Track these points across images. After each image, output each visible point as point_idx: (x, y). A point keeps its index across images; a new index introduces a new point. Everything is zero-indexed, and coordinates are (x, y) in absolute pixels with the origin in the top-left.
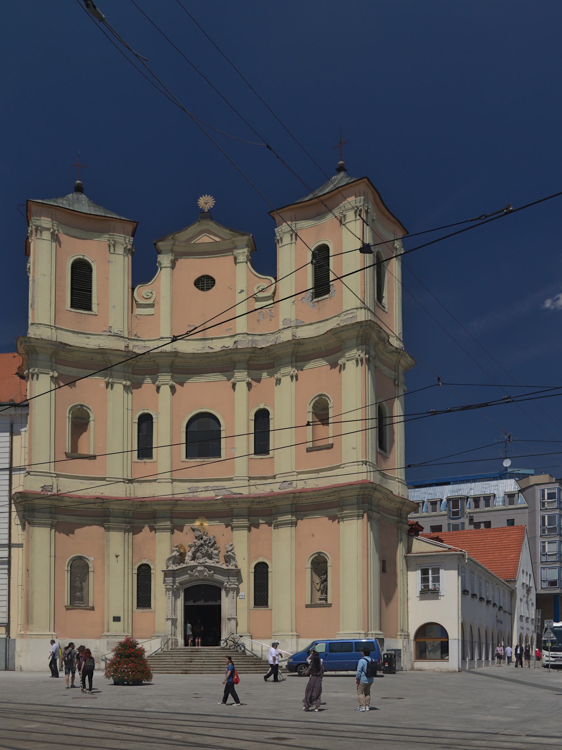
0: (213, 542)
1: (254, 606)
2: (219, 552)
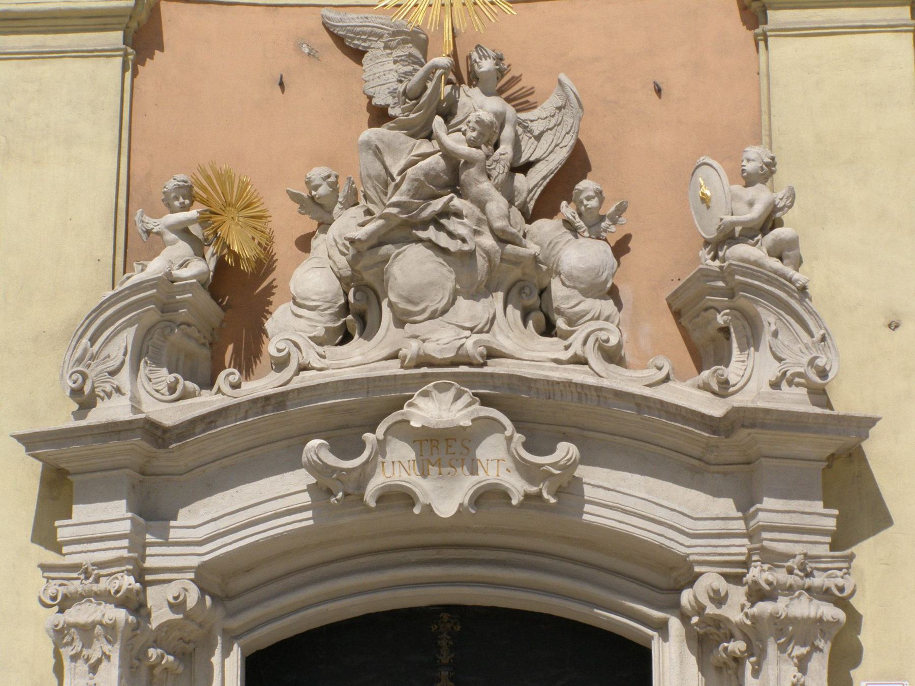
0: (561, 155)
2: (621, 248)
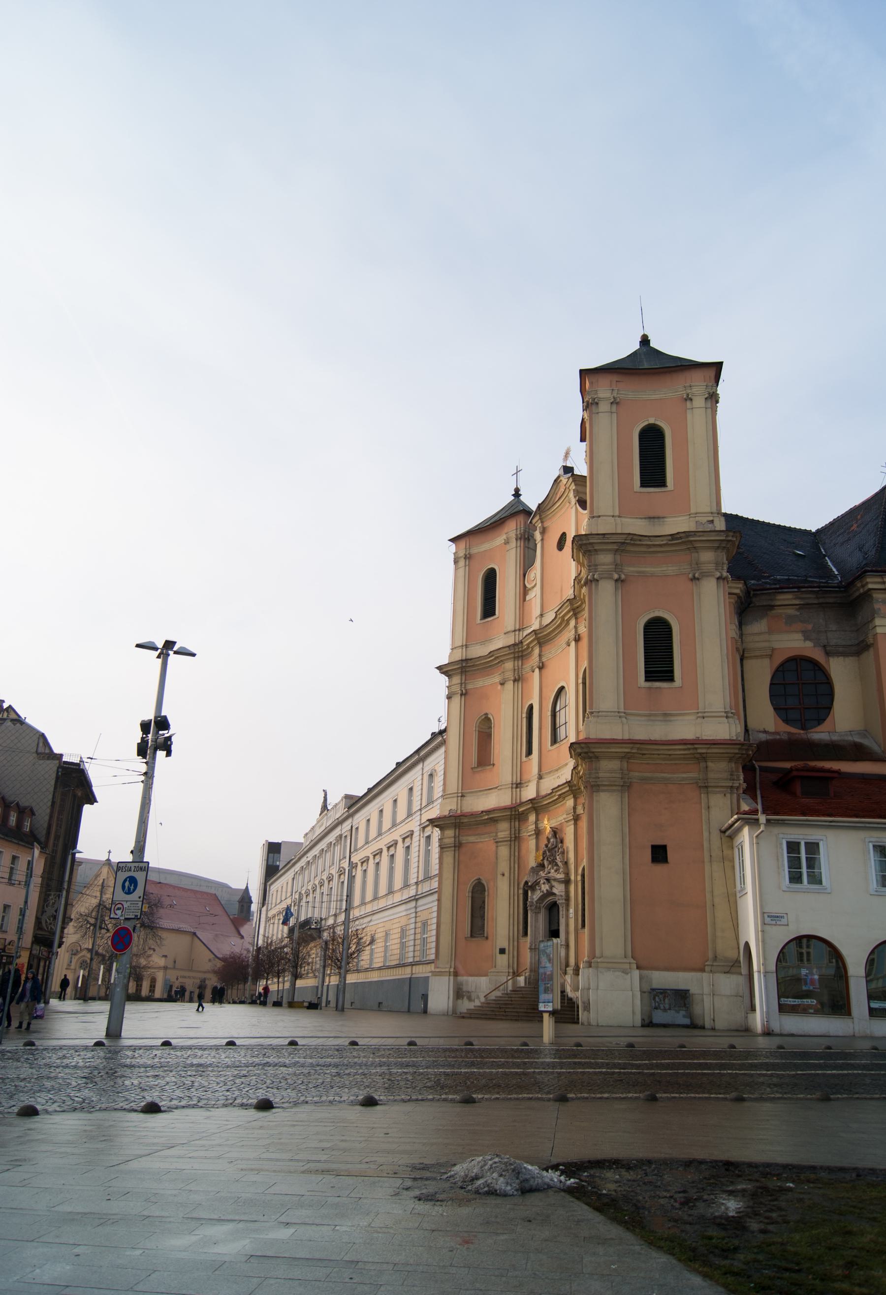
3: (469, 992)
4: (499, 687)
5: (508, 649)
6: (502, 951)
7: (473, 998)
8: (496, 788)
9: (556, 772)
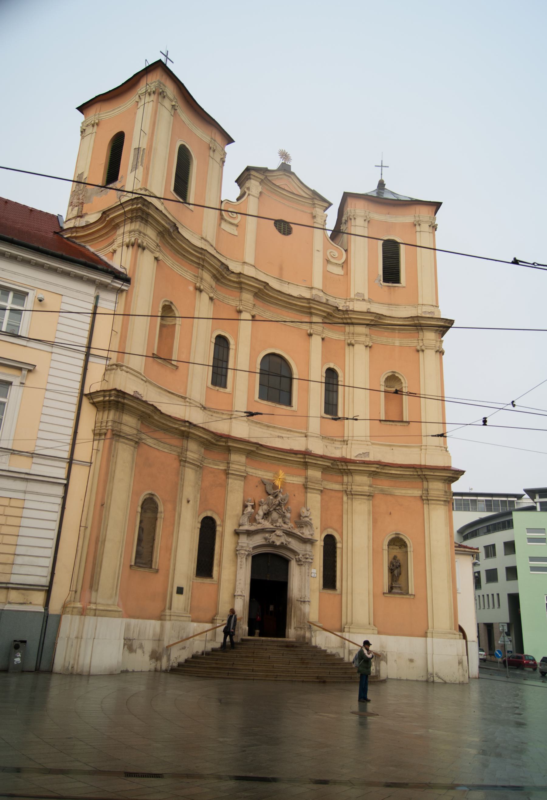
1: (322, 588)
3: (130, 640)
4: (191, 288)
5: (219, 264)
6: (180, 591)
7: (134, 647)
8: (182, 397)
9: (266, 428)
